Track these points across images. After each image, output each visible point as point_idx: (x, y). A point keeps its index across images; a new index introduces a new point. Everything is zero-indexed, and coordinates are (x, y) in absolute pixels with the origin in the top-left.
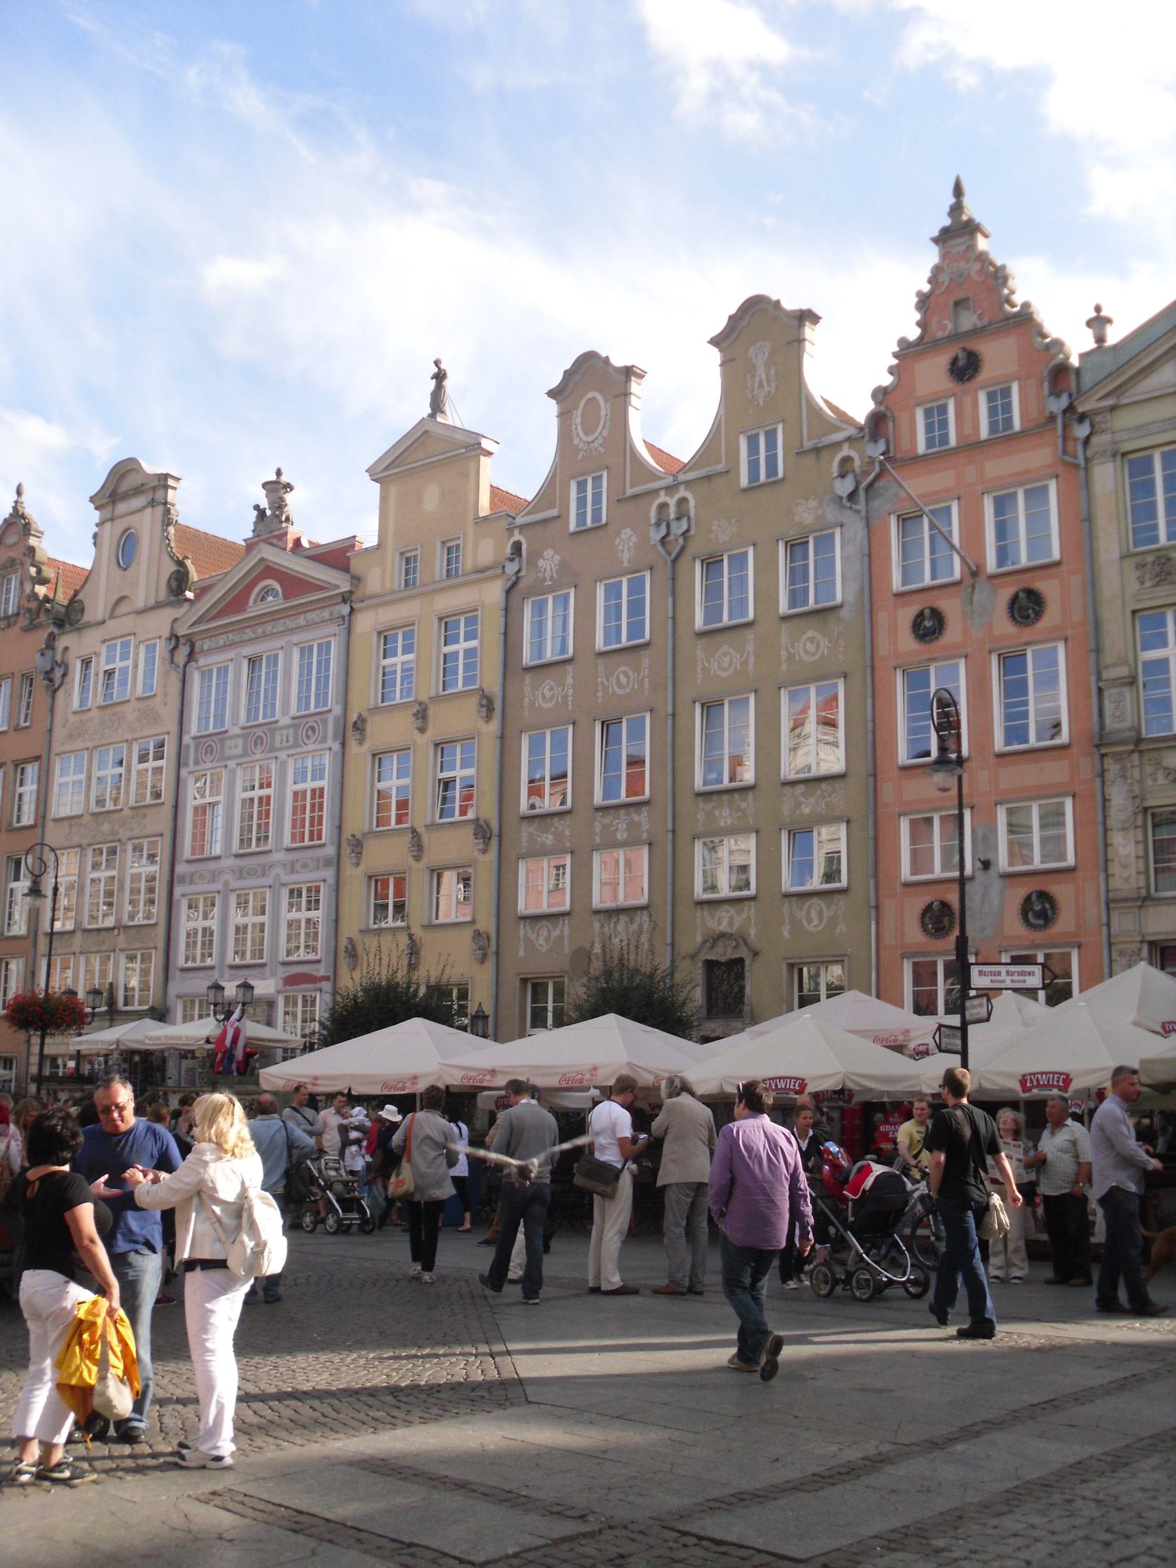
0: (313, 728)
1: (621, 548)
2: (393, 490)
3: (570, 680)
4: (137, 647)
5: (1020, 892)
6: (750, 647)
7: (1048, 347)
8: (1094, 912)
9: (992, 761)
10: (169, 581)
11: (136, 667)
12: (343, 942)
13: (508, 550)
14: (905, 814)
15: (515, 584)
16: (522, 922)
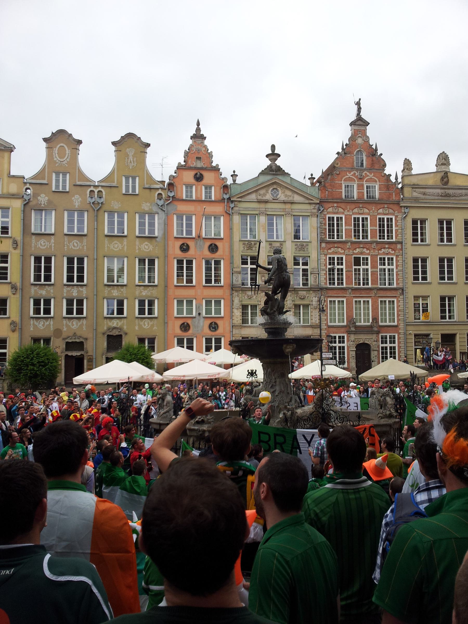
1: (74, 201)
5: (209, 322)
6: (125, 243)
7: (223, 179)
8: (228, 328)
9: (202, 287)
13: (24, 190)
14: (176, 299)
15: (28, 203)
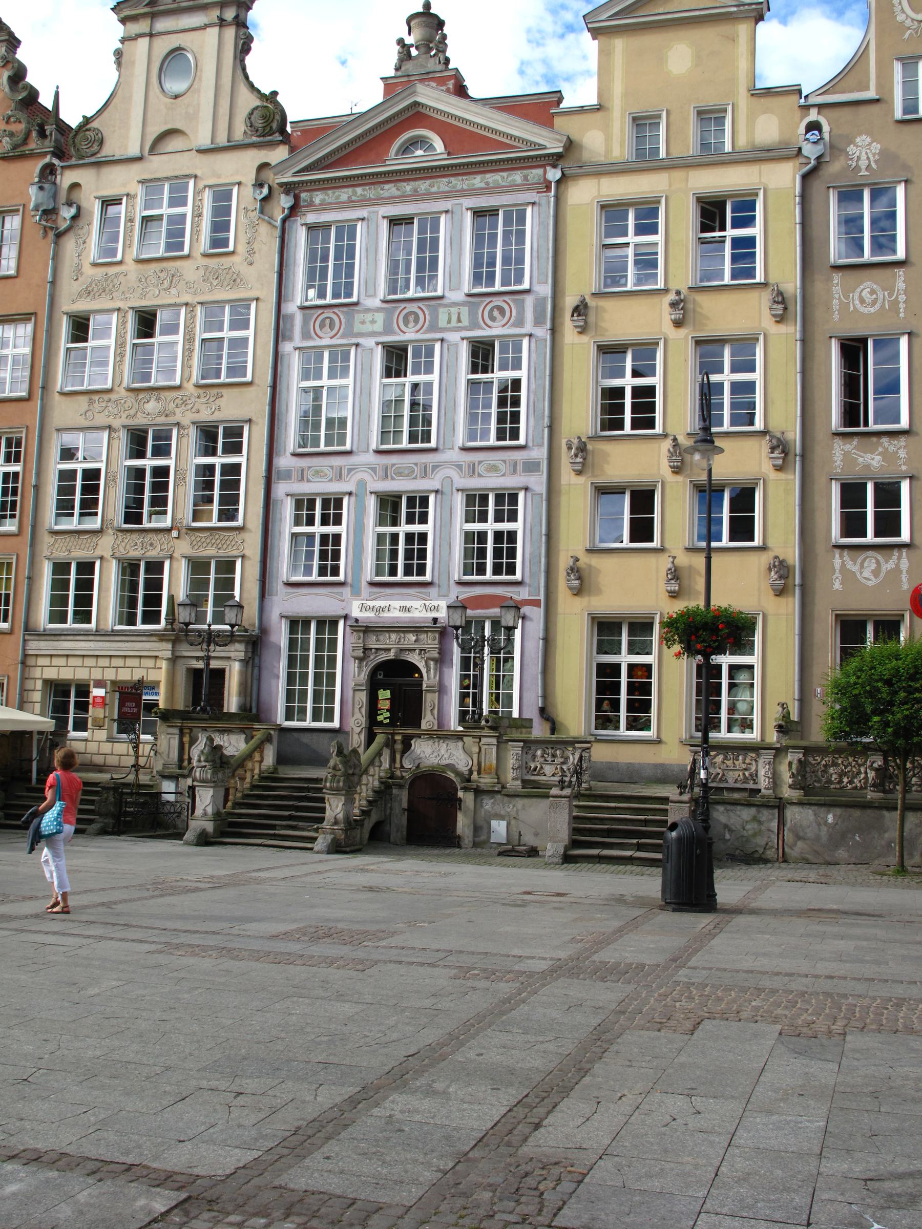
0: (502, 311)
2: (619, 44)
3: (901, 285)
4: (197, 193)
10: (251, 113)
11: (198, 215)
12: (563, 562)
16: (837, 551)
